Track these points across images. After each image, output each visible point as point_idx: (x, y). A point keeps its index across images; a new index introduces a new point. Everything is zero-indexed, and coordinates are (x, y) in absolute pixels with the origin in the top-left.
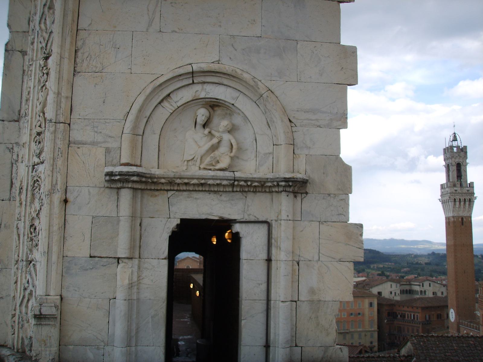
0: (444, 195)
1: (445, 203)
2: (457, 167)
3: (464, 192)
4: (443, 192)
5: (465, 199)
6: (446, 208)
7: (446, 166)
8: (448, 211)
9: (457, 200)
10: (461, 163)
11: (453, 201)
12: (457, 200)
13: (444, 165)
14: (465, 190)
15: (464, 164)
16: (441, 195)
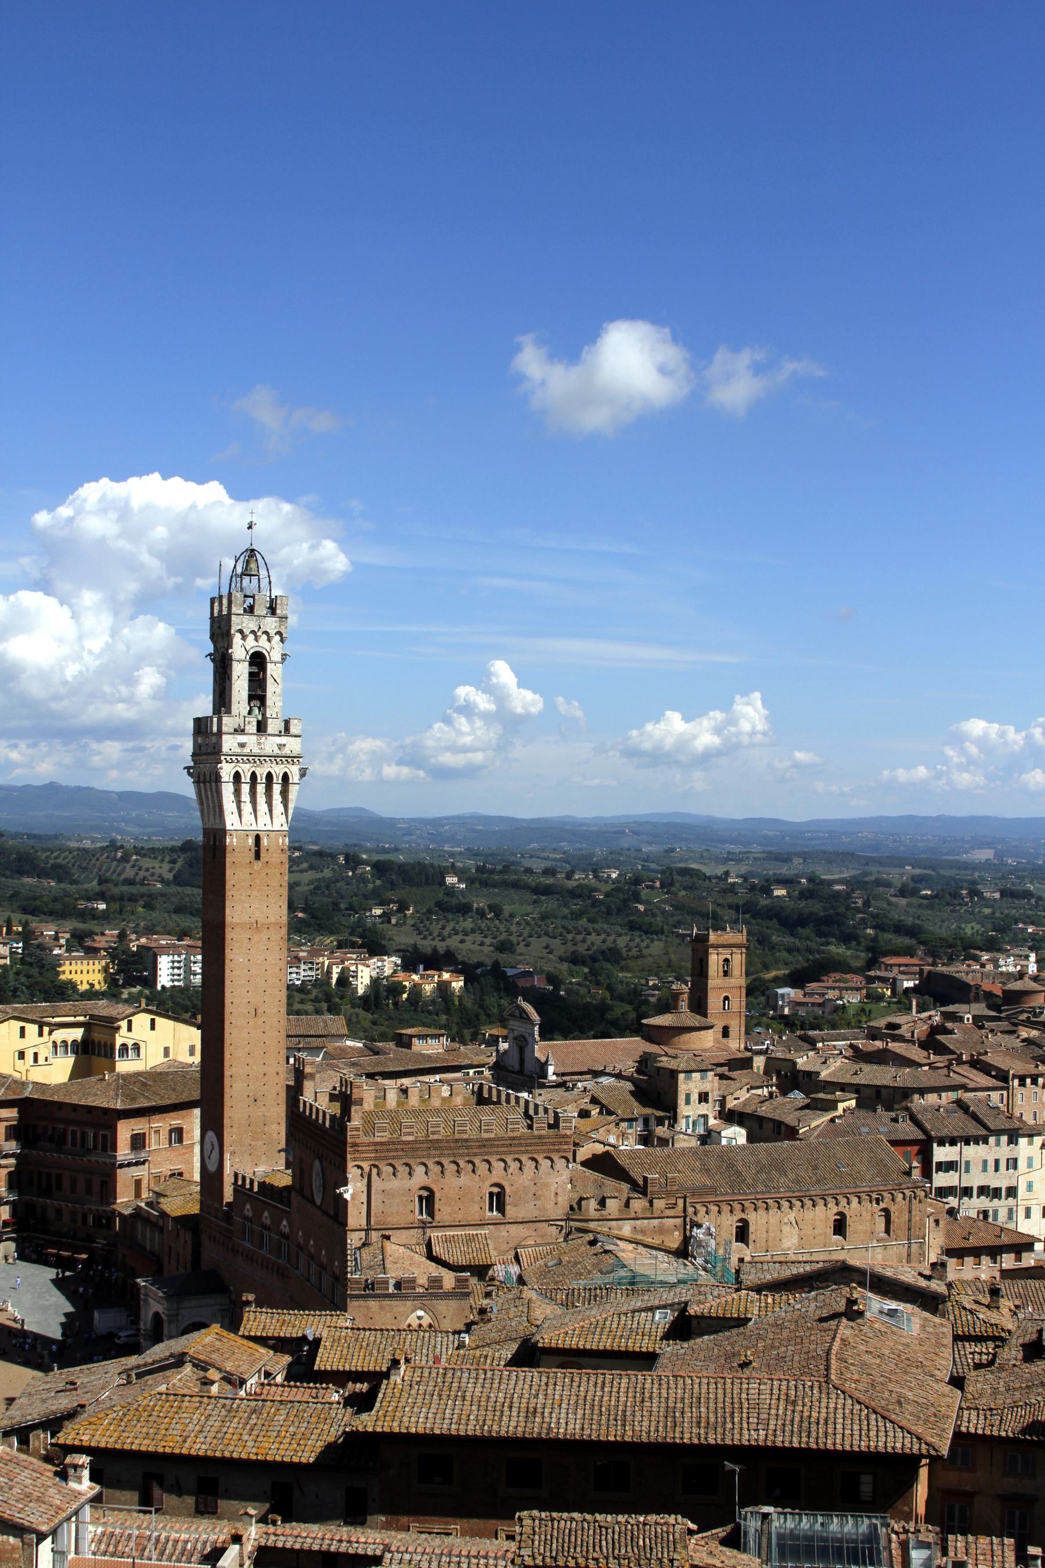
0: (204, 757)
1: (204, 782)
2: (251, 664)
3: (268, 750)
4: (200, 746)
5: (269, 776)
6: (207, 800)
7: (218, 658)
8: (215, 811)
9: (246, 778)
10: (265, 652)
11: (232, 780)
12: (246, 778)
13: (210, 655)
14: (270, 744)
15: (275, 655)
16: (194, 755)
